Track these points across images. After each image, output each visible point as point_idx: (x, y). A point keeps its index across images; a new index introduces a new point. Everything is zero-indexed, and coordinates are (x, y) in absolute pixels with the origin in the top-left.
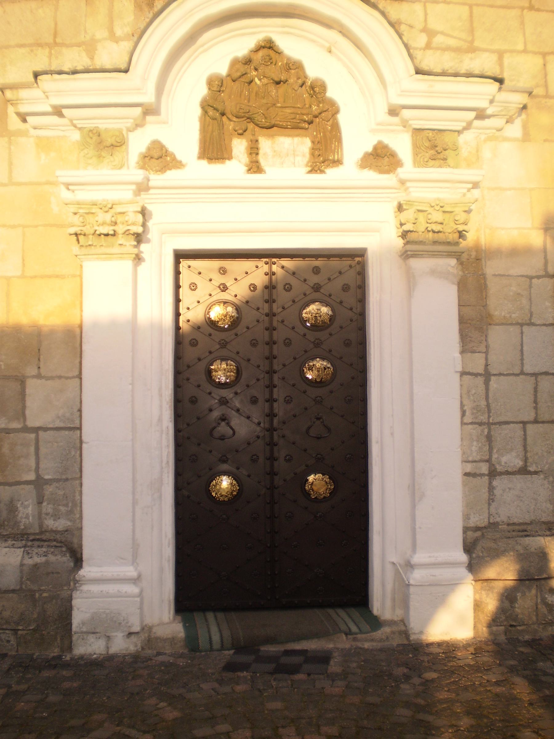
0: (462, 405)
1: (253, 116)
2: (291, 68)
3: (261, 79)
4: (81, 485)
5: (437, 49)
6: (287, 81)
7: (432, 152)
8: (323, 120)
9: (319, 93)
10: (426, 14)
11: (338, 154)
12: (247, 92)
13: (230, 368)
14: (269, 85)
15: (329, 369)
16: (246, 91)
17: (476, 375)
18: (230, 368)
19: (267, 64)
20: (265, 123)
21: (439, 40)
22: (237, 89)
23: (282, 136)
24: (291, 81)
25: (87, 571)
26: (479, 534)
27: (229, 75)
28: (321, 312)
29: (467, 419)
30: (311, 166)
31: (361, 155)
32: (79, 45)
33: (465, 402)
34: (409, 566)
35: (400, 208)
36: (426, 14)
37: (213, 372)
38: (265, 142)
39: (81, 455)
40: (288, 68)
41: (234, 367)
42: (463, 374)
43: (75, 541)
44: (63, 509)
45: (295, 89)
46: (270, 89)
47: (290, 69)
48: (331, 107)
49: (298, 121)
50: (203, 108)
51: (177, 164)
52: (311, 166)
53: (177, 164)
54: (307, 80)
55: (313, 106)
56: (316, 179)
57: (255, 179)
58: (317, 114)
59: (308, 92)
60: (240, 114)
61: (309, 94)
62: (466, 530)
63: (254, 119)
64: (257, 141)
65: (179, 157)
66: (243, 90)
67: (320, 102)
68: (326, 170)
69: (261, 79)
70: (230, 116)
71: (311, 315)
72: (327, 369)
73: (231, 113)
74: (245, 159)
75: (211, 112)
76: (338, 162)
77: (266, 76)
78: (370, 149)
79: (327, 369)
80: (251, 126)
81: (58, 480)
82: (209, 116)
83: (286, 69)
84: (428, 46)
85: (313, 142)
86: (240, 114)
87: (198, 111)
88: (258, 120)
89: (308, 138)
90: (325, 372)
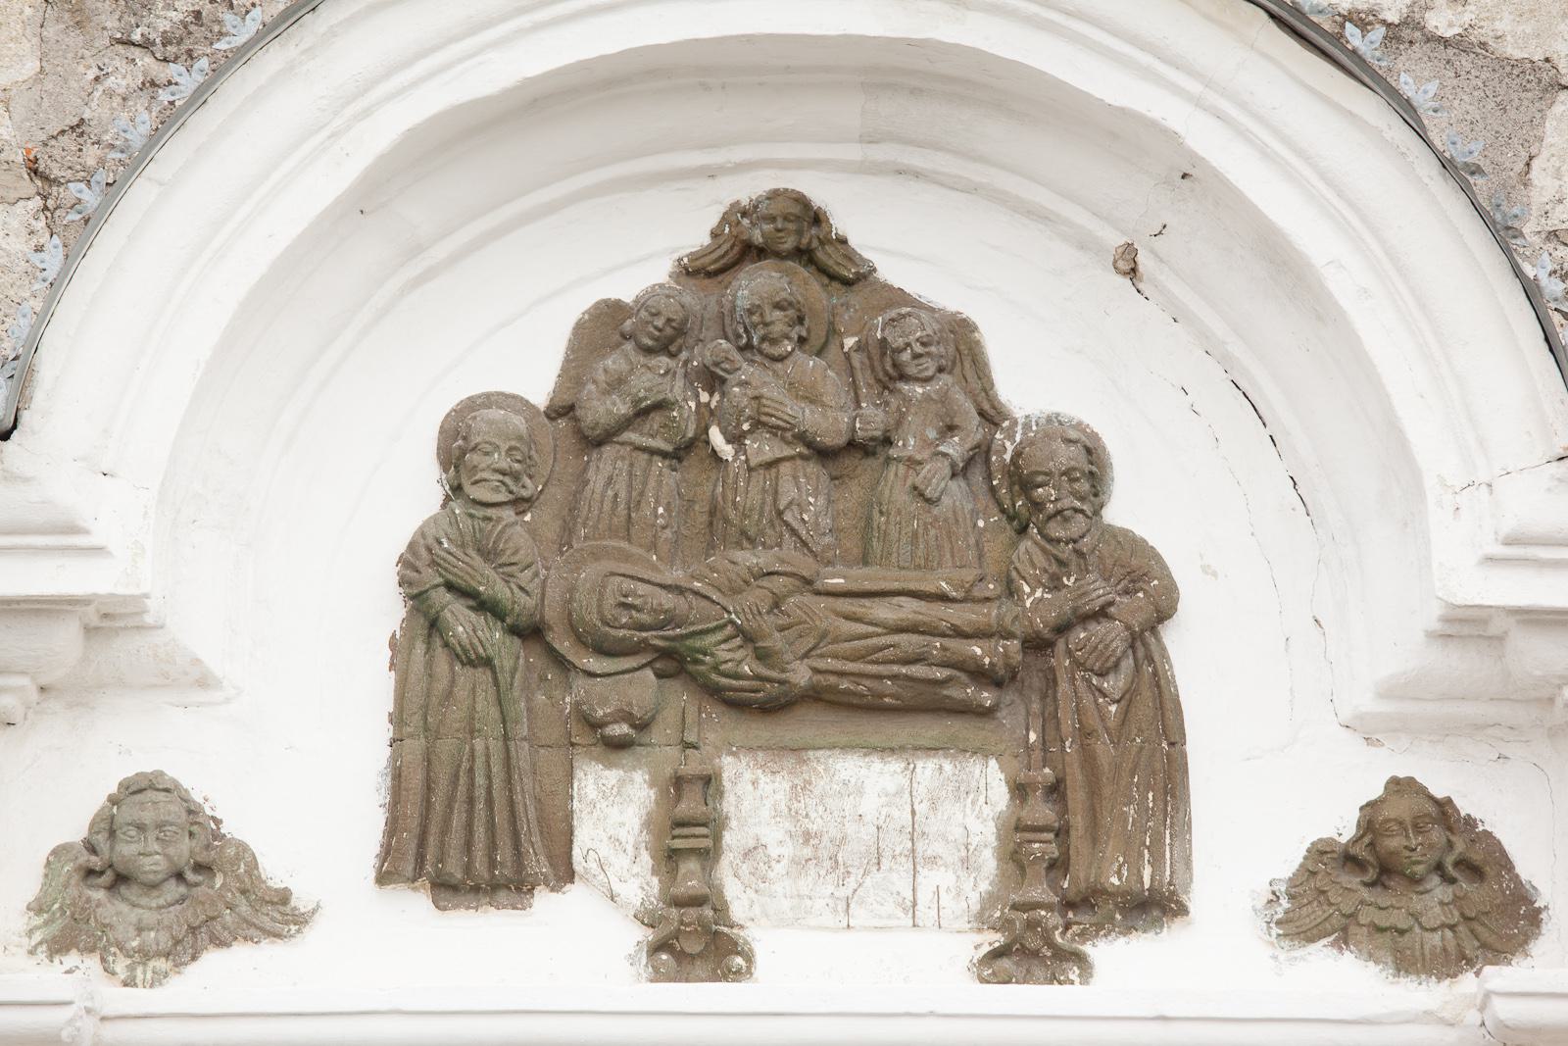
1: (689, 642)
2: (912, 370)
3: (743, 435)
6: (887, 441)
8: (1078, 664)
9: (1059, 512)
11: (1157, 861)
12: (661, 510)
14: (785, 468)
16: (657, 503)
19: (776, 351)
20: (755, 684)
22: (610, 493)
23: (847, 748)
24: (908, 445)
27: (562, 410)
30: (1004, 925)
31: (1288, 861)
38: (754, 783)
40: (889, 368)
45: (928, 493)
46: (788, 492)
47: (903, 377)
48: (1126, 592)
49: (939, 674)
52: (1004, 925)
54: (998, 436)
55: (1027, 589)
58: (1046, 633)
59: (999, 503)
60: (622, 633)
61: (1003, 511)
63: (696, 662)
64: (709, 782)
65: (275, 870)
66: (642, 494)
67: (1061, 563)
68: (1087, 948)
69: (743, 435)
70: (564, 645)
73: (573, 628)
75: (462, 622)
77: (764, 418)
78: (1343, 827)
80: (680, 698)
82: (446, 645)
83: (881, 375)
85: (1020, 791)
86: (622, 633)
87: (390, 611)
88: (715, 668)
89: (993, 763)
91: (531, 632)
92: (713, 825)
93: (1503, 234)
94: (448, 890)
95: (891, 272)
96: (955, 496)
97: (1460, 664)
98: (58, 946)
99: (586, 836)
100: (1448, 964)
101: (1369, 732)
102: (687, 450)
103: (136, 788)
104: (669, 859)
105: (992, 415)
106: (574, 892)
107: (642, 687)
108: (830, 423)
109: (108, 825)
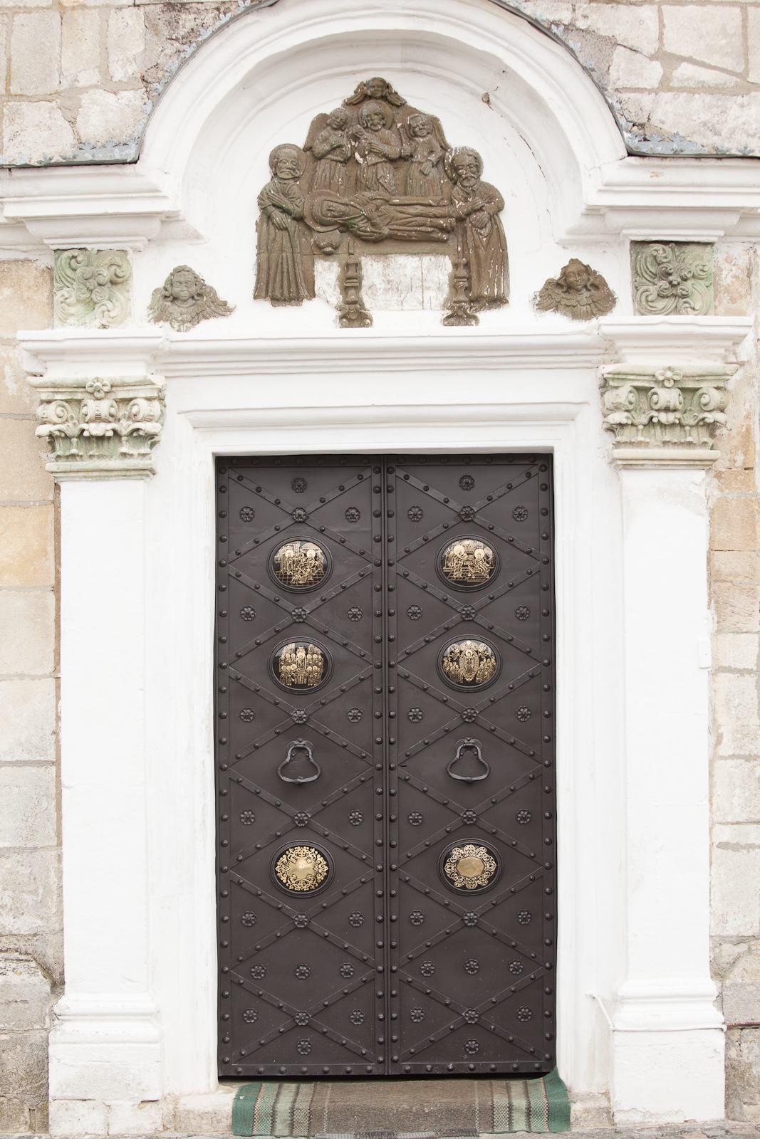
0: (714, 726)
1: (350, 221)
2: (419, 134)
3: (366, 155)
4: (60, 858)
5: (681, 90)
6: (412, 156)
7: (664, 284)
8: (473, 226)
9: (466, 178)
10: (662, 25)
11: (499, 287)
12: (340, 180)
13: (312, 659)
14: (379, 165)
15: (489, 660)
16: (339, 177)
17: (742, 672)
18: (312, 659)
19: (376, 128)
20: (372, 234)
21: (685, 70)
22: (324, 175)
23: (401, 253)
24: (418, 157)
25: (67, 1002)
26: (743, 947)
27: (308, 148)
28: (475, 558)
29: (726, 748)
30: (451, 308)
31: (540, 285)
32: (49, 98)
33: (722, 719)
34: (618, 1001)
35: (605, 385)
36: (662, 25)
37: (281, 665)
38: (372, 265)
39: (59, 808)
40: (412, 133)
41: (320, 657)
42: (718, 670)
43: (50, 952)
44: (29, 898)
45: (425, 173)
46: (381, 173)
47: (416, 136)
48: (488, 202)
49: (429, 230)
50: (266, 217)
51: (222, 309)
52: (451, 308)
53: (222, 309)
54: (447, 154)
55: (457, 202)
56: (461, 334)
57: (356, 334)
58: (463, 216)
59: (448, 175)
60: (329, 219)
61: (449, 178)
62: (718, 941)
63: (352, 227)
64: (357, 265)
65: (222, 295)
66: (334, 174)
67: (468, 194)
68: (477, 314)
69: (366, 155)
70: (311, 223)
71: (456, 564)
72: (485, 660)
73: (313, 218)
74: (335, 297)
75: (278, 217)
76: (498, 301)
77: (372, 150)
78: (556, 274)
79: (485, 660)
80: (347, 239)
81: (20, 850)
82: (273, 224)
83: (409, 135)
84: (665, 85)
85: (456, 266)
86: (329, 219)
87: (255, 213)
88: (359, 229)
89: (447, 257)
90: (482, 665)
91: (300, 219)
92: (359, 279)
93: (602, 90)
94: (276, 300)
95: (411, 103)
96: (434, 173)
97: (590, 223)
98: (157, 319)
99: (320, 284)
100: (589, 316)
101: (564, 245)
102: (348, 160)
103: (179, 271)
104: (345, 290)
105: (445, 147)
106: (315, 300)
107: (335, 236)
108: (393, 151)
109: (170, 282)
